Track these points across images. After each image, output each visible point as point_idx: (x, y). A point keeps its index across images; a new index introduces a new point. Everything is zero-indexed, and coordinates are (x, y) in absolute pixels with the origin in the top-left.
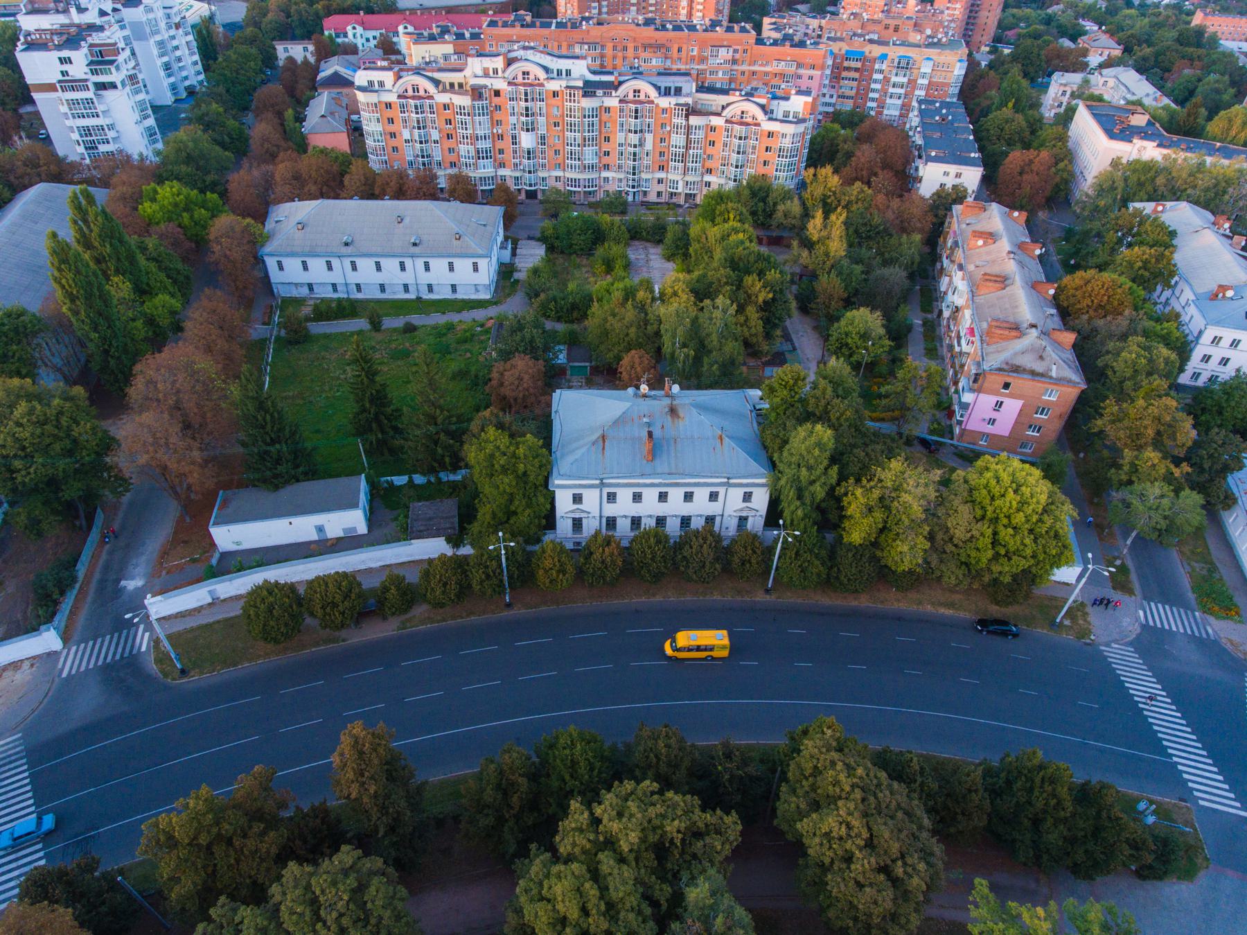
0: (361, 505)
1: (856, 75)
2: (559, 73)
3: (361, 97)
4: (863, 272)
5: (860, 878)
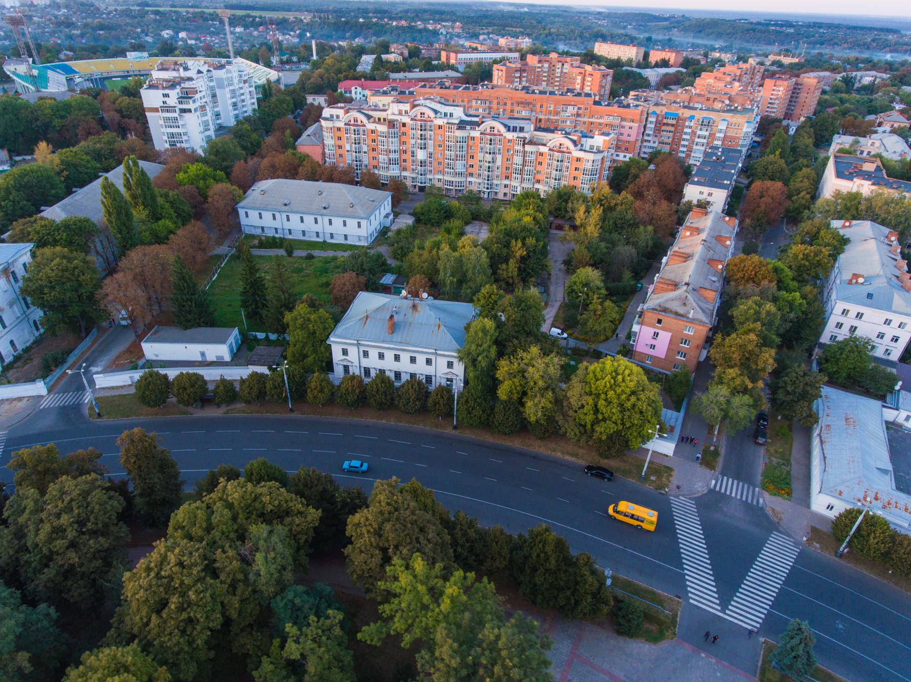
0: (229, 342)
1: (672, 129)
2: (446, 115)
3: (323, 123)
4: (607, 248)
5: (363, 548)
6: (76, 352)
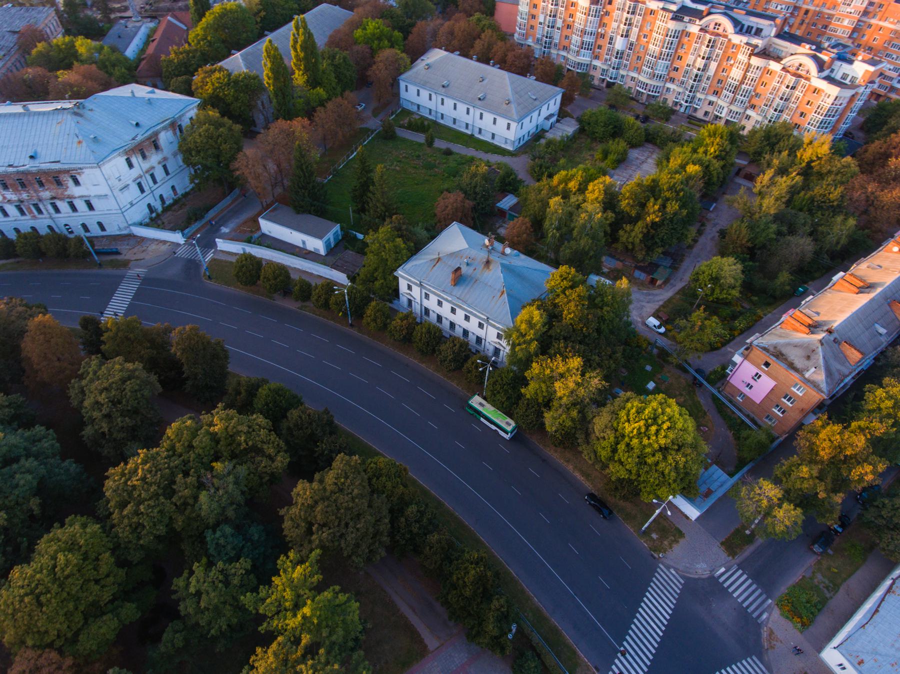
0: (326, 238)
6: (215, 208)
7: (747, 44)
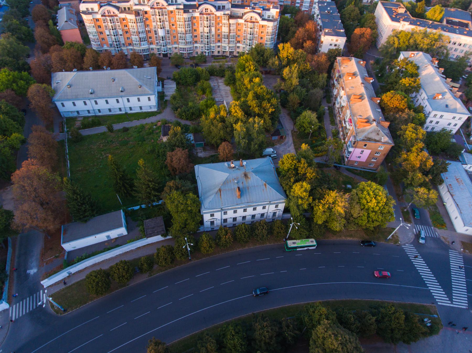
0: (124, 225)
7: (224, 14)
